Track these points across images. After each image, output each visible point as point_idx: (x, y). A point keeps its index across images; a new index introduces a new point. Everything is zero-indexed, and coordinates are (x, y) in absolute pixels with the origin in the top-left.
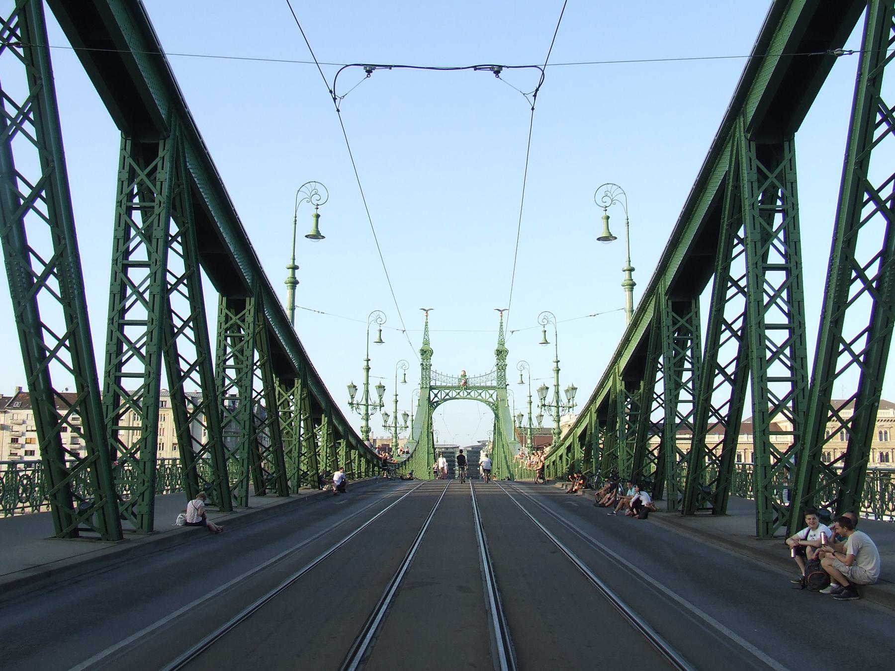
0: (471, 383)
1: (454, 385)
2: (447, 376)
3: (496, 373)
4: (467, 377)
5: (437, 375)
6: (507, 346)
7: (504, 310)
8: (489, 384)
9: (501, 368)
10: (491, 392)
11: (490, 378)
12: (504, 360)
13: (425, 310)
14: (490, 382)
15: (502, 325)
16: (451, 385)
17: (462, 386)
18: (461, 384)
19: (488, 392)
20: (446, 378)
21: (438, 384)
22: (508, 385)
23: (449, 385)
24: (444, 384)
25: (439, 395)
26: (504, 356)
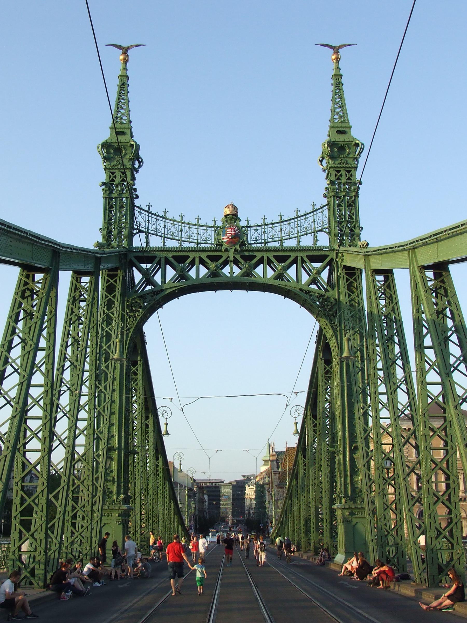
1: (203, 246)
2: (182, 222)
3: (326, 212)
4: (243, 223)
5: (153, 220)
8: (307, 242)
11: (306, 223)
13: (119, 47)
15: (339, 83)
16: (192, 245)
17: (226, 245)
18: (225, 239)
20: (178, 227)
21: (155, 242)
23: (186, 245)
25: (158, 278)
26: (350, 161)
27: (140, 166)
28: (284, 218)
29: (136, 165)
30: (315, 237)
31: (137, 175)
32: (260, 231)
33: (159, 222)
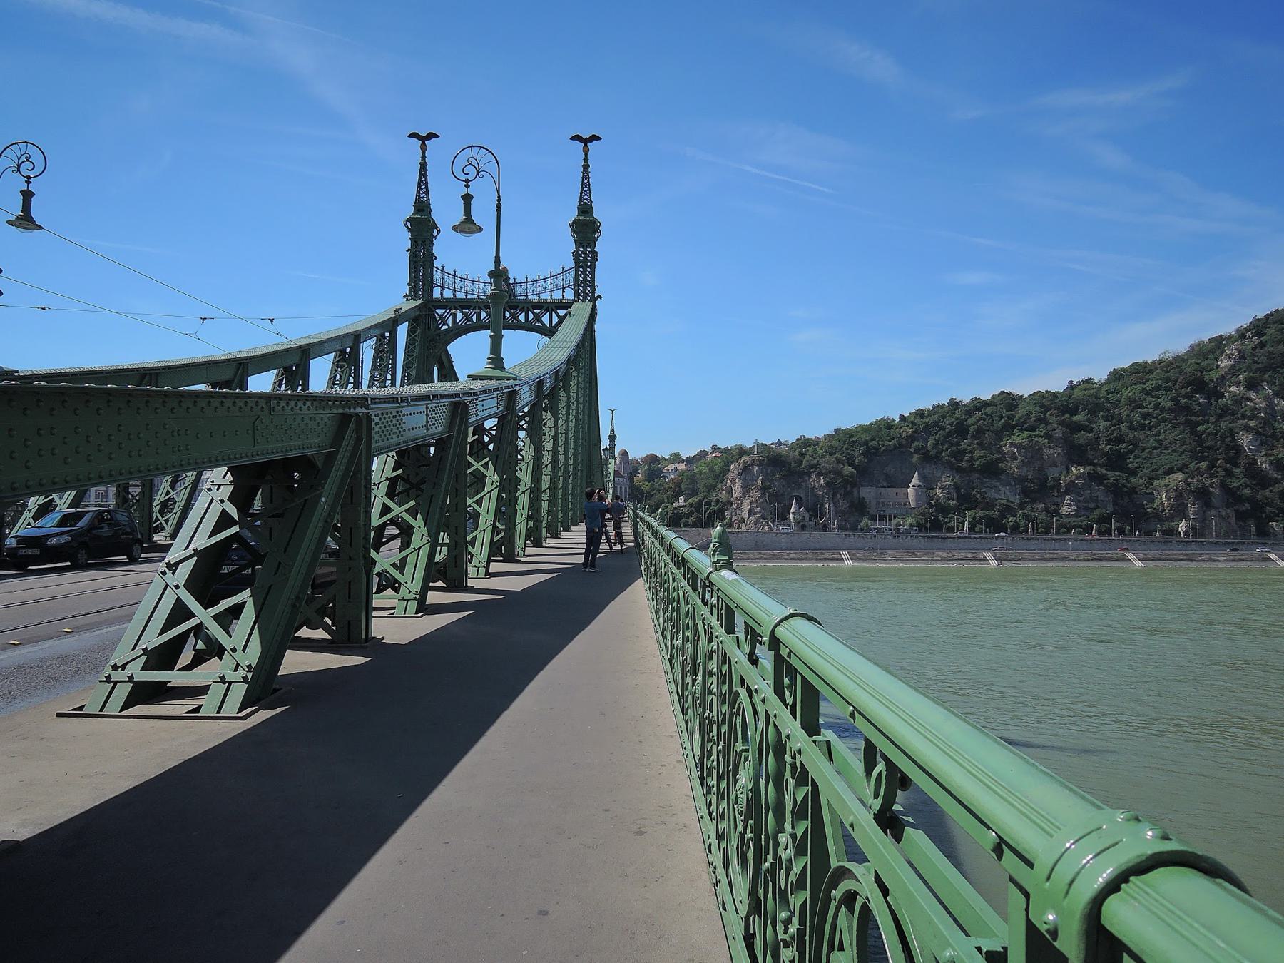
0: (520, 292)
3: (573, 273)
5: (446, 276)
6: (596, 215)
7: (594, 138)
8: (557, 295)
9: (585, 259)
10: (562, 313)
11: (557, 281)
12: (592, 243)
14: (560, 292)
16: (475, 297)
19: (557, 315)
21: (448, 294)
22: (600, 297)
24: (460, 296)
27: (438, 234)
28: (541, 278)
29: (435, 234)
30: (563, 292)
31: (435, 241)
32: (524, 286)
33: (451, 279)
